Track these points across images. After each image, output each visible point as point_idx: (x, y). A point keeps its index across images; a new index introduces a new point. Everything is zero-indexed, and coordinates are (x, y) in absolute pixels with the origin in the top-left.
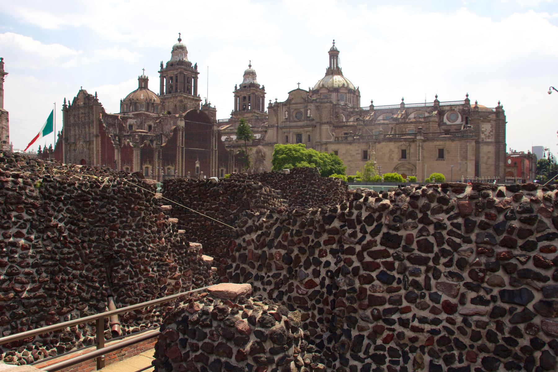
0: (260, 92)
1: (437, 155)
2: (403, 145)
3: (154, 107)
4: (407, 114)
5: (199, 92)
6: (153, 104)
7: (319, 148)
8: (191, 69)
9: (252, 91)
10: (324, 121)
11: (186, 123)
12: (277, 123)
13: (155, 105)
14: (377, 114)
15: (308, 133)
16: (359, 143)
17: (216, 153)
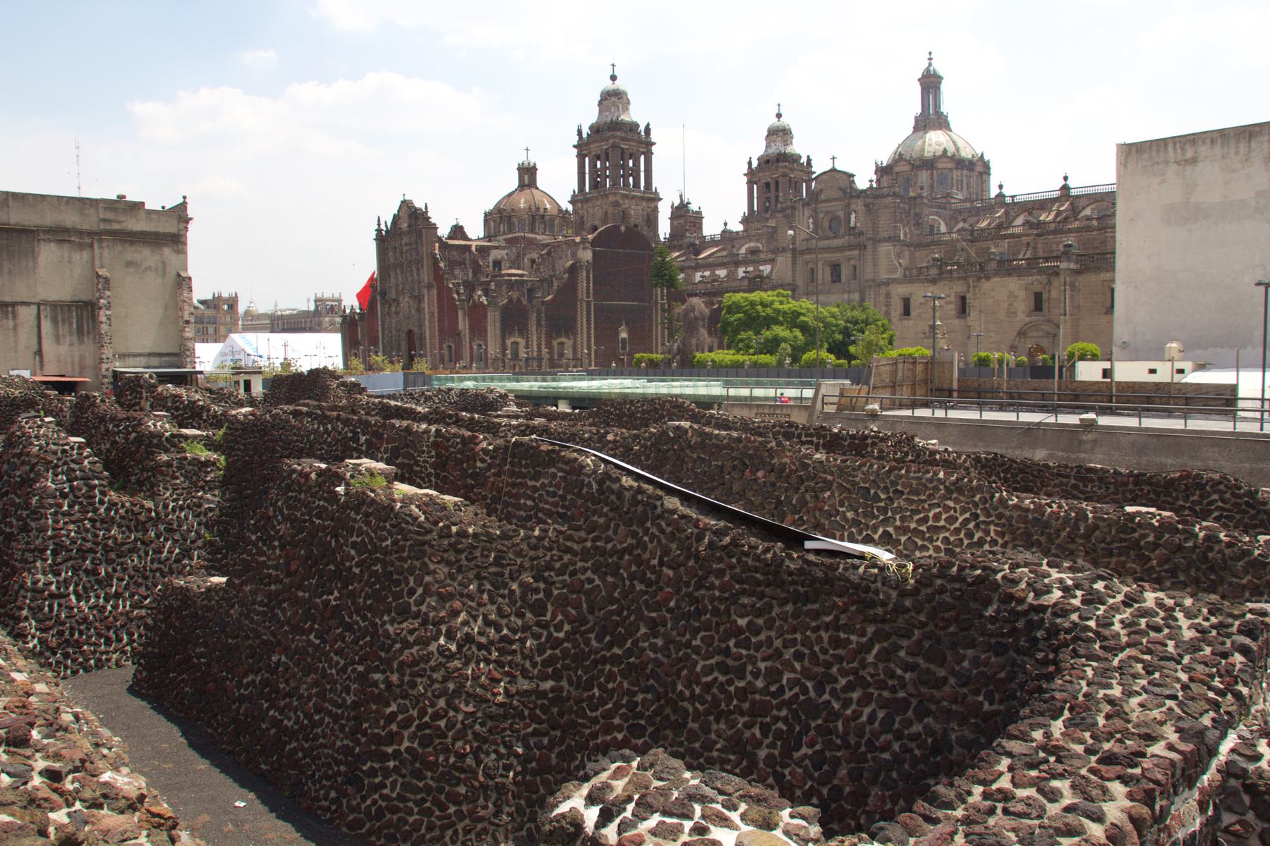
4: (1075, 211)
5: (655, 183)
6: (543, 216)
7: (872, 293)
9: (781, 170)
10: (883, 234)
11: (595, 254)
14: (1012, 212)
15: (853, 262)
16: (951, 279)
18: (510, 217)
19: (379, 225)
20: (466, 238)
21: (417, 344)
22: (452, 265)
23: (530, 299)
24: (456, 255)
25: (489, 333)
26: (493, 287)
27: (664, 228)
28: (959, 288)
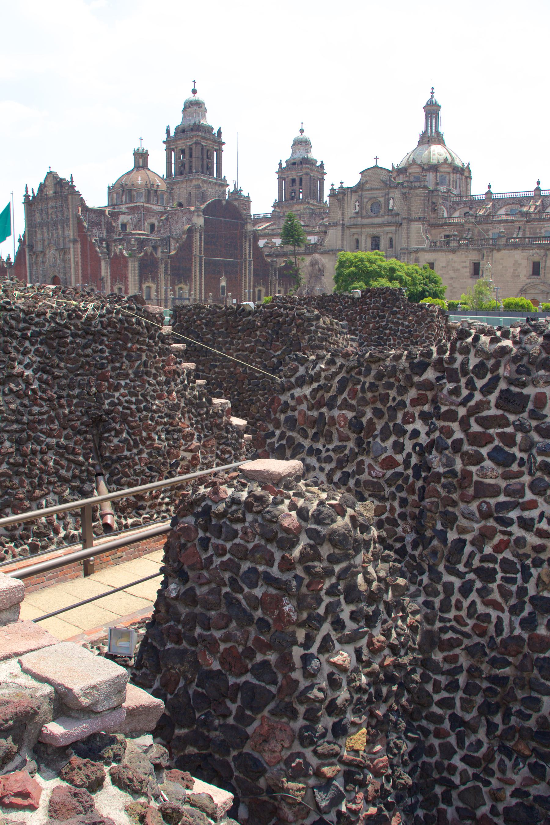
0: (318, 172)
3: (157, 196)
6: (156, 191)
7: (406, 258)
8: (212, 137)
9: (304, 171)
11: (206, 220)
12: (343, 220)
13: (159, 193)
14: (497, 205)
15: (390, 235)
17: (250, 265)
28: (474, 257)
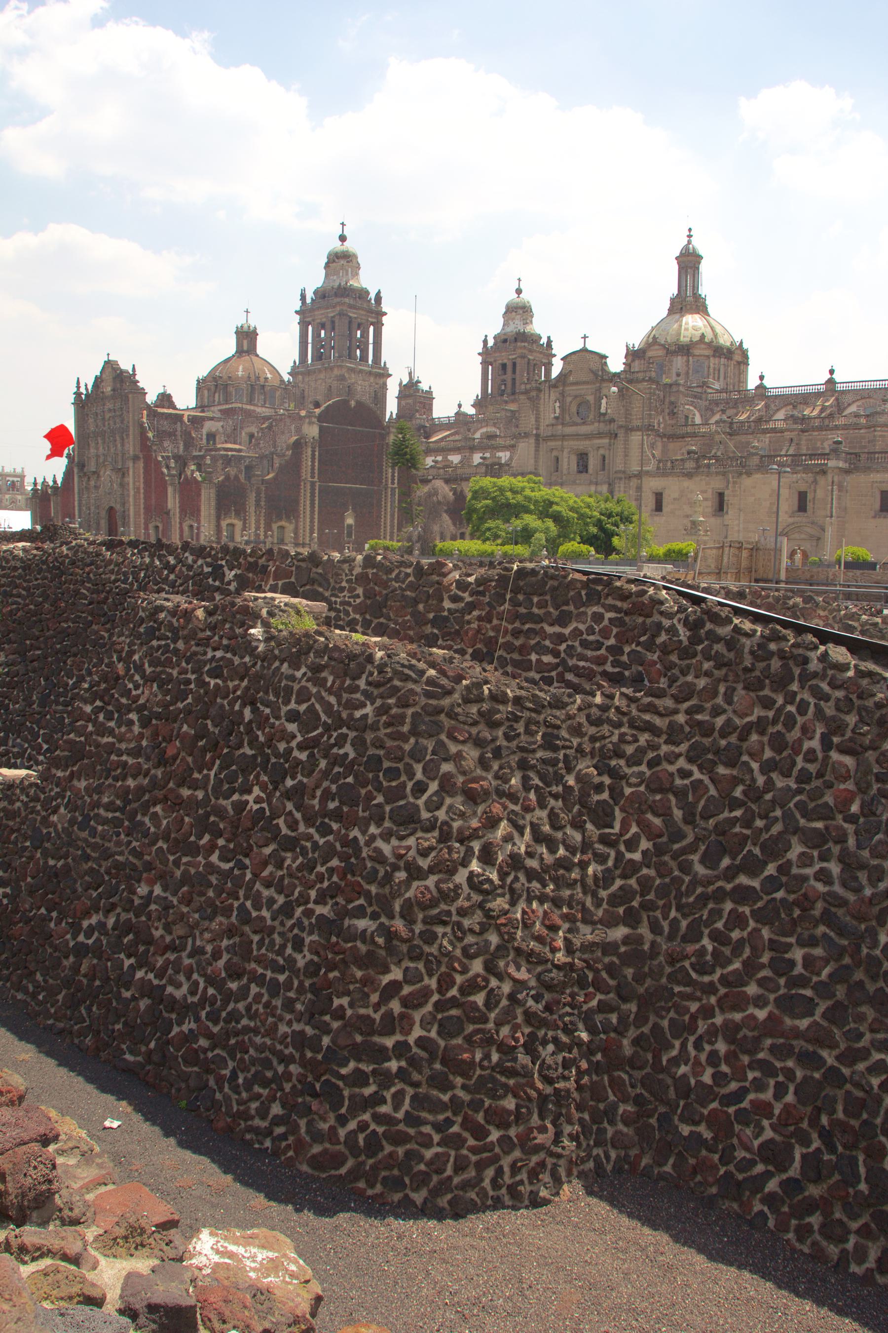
0: (541, 353)
1: (877, 505)
2: (801, 480)
3: (265, 394)
4: (840, 407)
5: (385, 357)
6: (263, 387)
7: (622, 485)
8: (365, 306)
9: (519, 351)
10: (637, 423)
11: (321, 429)
12: (537, 429)
13: (267, 389)
14: (772, 406)
15: (602, 452)
18: (226, 386)
19: (78, 387)
20: (175, 408)
21: (119, 523)
22: (161, 435)
23: (248, 478)
24: (166, 425)
25: (204, 513)
26: (208, 462)
27: (392, 407)
28: (717, 483)
